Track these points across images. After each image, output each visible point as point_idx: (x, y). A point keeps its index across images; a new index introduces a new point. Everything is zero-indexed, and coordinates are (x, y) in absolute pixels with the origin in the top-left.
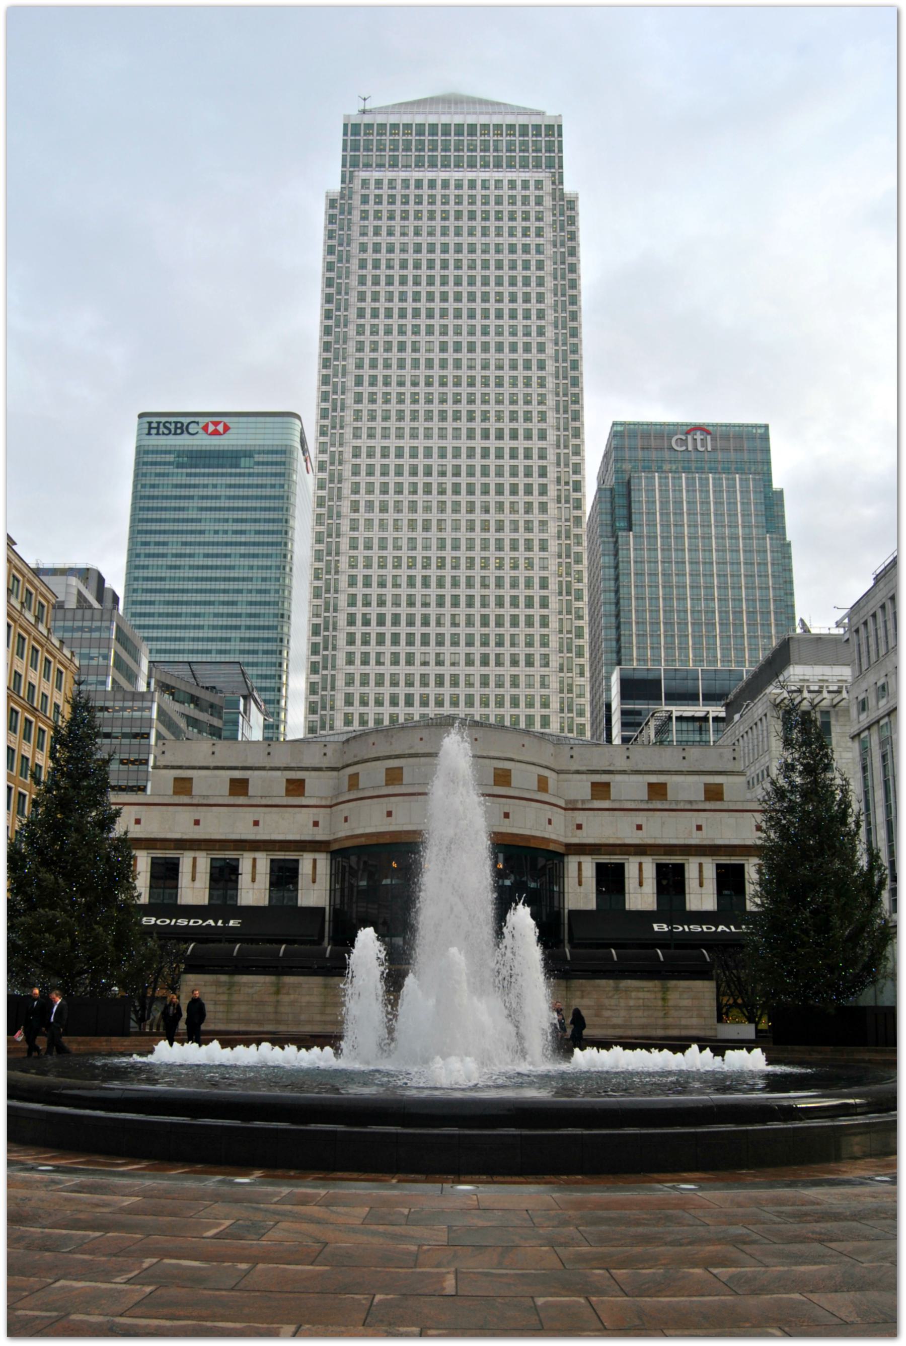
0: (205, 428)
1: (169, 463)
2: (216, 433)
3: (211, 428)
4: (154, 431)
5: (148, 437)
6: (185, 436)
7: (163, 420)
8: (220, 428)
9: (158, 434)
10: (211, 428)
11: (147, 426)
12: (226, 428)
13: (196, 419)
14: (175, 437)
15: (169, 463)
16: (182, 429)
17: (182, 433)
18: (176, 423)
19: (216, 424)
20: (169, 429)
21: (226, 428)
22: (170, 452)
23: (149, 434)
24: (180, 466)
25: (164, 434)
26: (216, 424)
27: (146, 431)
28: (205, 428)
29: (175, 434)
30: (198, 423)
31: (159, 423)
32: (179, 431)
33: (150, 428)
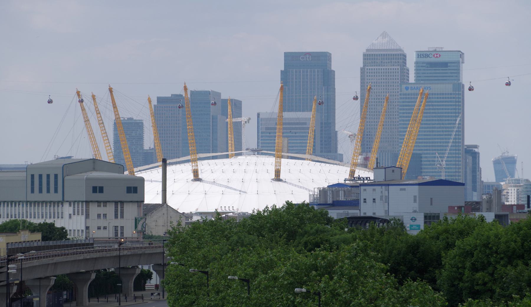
1: (424, 66)
2: (437, 57)
3: (436, 56)
4: (419, 57)
6: (429, 58)
7: (422, 53)
9: (421, 57)
10: (436, 56)
12: (440, 56)
13: (431, 53)
15: (424, 66)
16: (427, 56)
17: (427, 57)
18: (426, 54)
19: (437, 54)
22: (425, 63)
24: (428, 67)
25: (422, 57)
26: (438, 54)
29: (426, 57)
31: (421, 54)
32: (426, 57)
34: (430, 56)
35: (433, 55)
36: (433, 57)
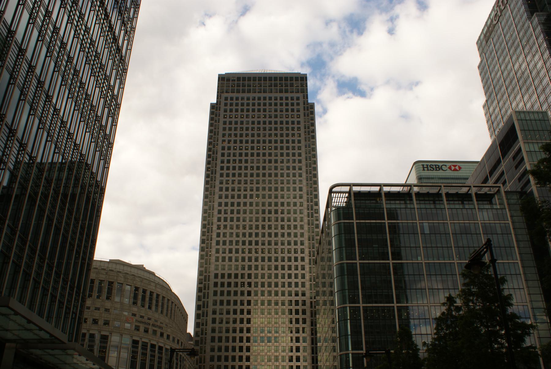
0: (450, 168)
2: (455, 170)
3: (453, 168)
5: (424, 171)
8: (457, 168)
10: (453, 168)
11: (422, 166)
14: (436, 172)
18: (436, 165)
19: (455, 166)
20: (431, 167)
21: (460, 168)
23: (424, 170)
25: (431, 170)
27: (422, 169)
28: (450, 168)
29: (436, 170)
30: (446, 166)
33: (424, 168)
34: (444, 168)
35: (448, 167)
36: (448, 169)
